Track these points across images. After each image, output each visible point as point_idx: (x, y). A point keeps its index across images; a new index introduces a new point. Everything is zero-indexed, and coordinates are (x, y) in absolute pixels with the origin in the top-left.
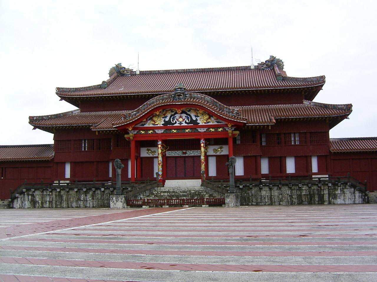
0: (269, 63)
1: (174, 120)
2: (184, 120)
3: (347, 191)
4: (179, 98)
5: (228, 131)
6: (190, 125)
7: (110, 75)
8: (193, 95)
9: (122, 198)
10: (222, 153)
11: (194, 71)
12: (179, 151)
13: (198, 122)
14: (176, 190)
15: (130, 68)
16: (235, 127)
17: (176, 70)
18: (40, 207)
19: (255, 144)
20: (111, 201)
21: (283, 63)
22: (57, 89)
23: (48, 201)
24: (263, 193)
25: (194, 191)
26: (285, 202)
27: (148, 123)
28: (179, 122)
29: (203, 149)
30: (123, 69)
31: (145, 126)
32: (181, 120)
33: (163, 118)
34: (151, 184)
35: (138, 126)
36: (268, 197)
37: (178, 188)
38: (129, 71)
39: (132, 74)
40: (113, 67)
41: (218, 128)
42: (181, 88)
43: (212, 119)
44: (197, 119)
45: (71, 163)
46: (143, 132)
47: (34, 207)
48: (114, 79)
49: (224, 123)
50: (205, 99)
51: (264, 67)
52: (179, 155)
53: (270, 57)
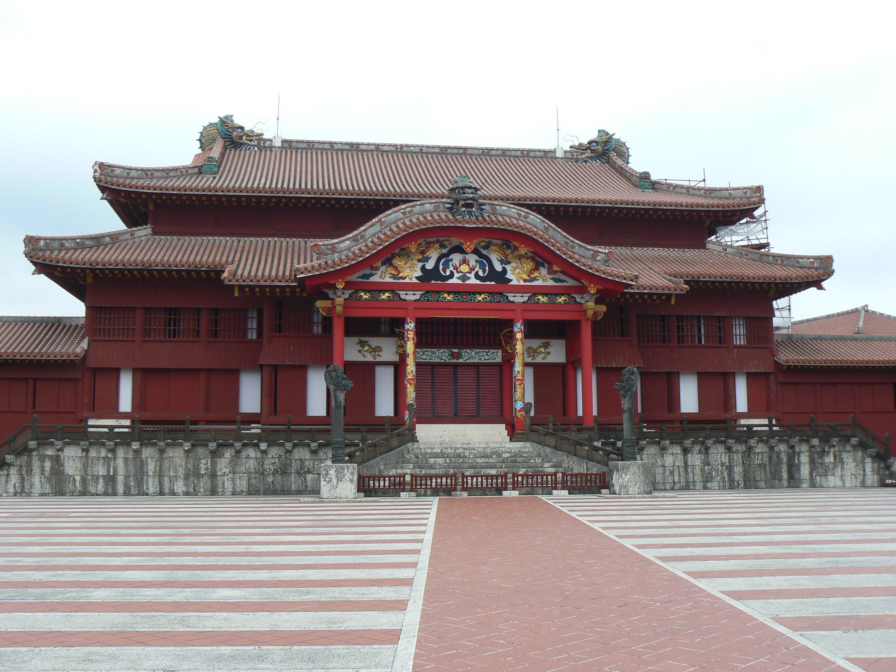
0: (599, 147)
1: (449, 268)
2: (472, 269)
3: (848, 458)
4: (470, 213)
5: (580, 303)
6: (488, 283)
7: (202, 143)
8: (498, 207)
9: (351, 471)
10: (550, 359)
11: (421, 150)
12: (442, 351)
13: (509, 276)
14: (461, 450)
15: (257, 131)
16: (598, 295)
17: (374, 144)
18: (76, 494)
19: (628, 339)
20: (322, 480)
21: (627, 149)
22: (96, 167)
23: (104, 476)
24: (669, 460)
25: (508, 452)
26: (717, 484)
27: (379, 273)
28: (461, 274)
29: (519, 347)
30: (240, 130)
31: (373, 279)
32: (464, 268)
33: (419, 261)
34: (398, 435)
35: (354, 278)
36: (679, 471)
37: (464, 446)
38: (254, 138)
39: (261, 144)
40: (211, 124)
41: (557, 295)
42: (470, 188)
43: (544, 271)
44: (504, 270)
45: (135, 371)
46: (365, 297)
47: (59, 492)
48: (223, 155)
49: (571, 282)
50: (528, 220)
51: (587, 155)
52: (443, 361)
53: (597, 134)
